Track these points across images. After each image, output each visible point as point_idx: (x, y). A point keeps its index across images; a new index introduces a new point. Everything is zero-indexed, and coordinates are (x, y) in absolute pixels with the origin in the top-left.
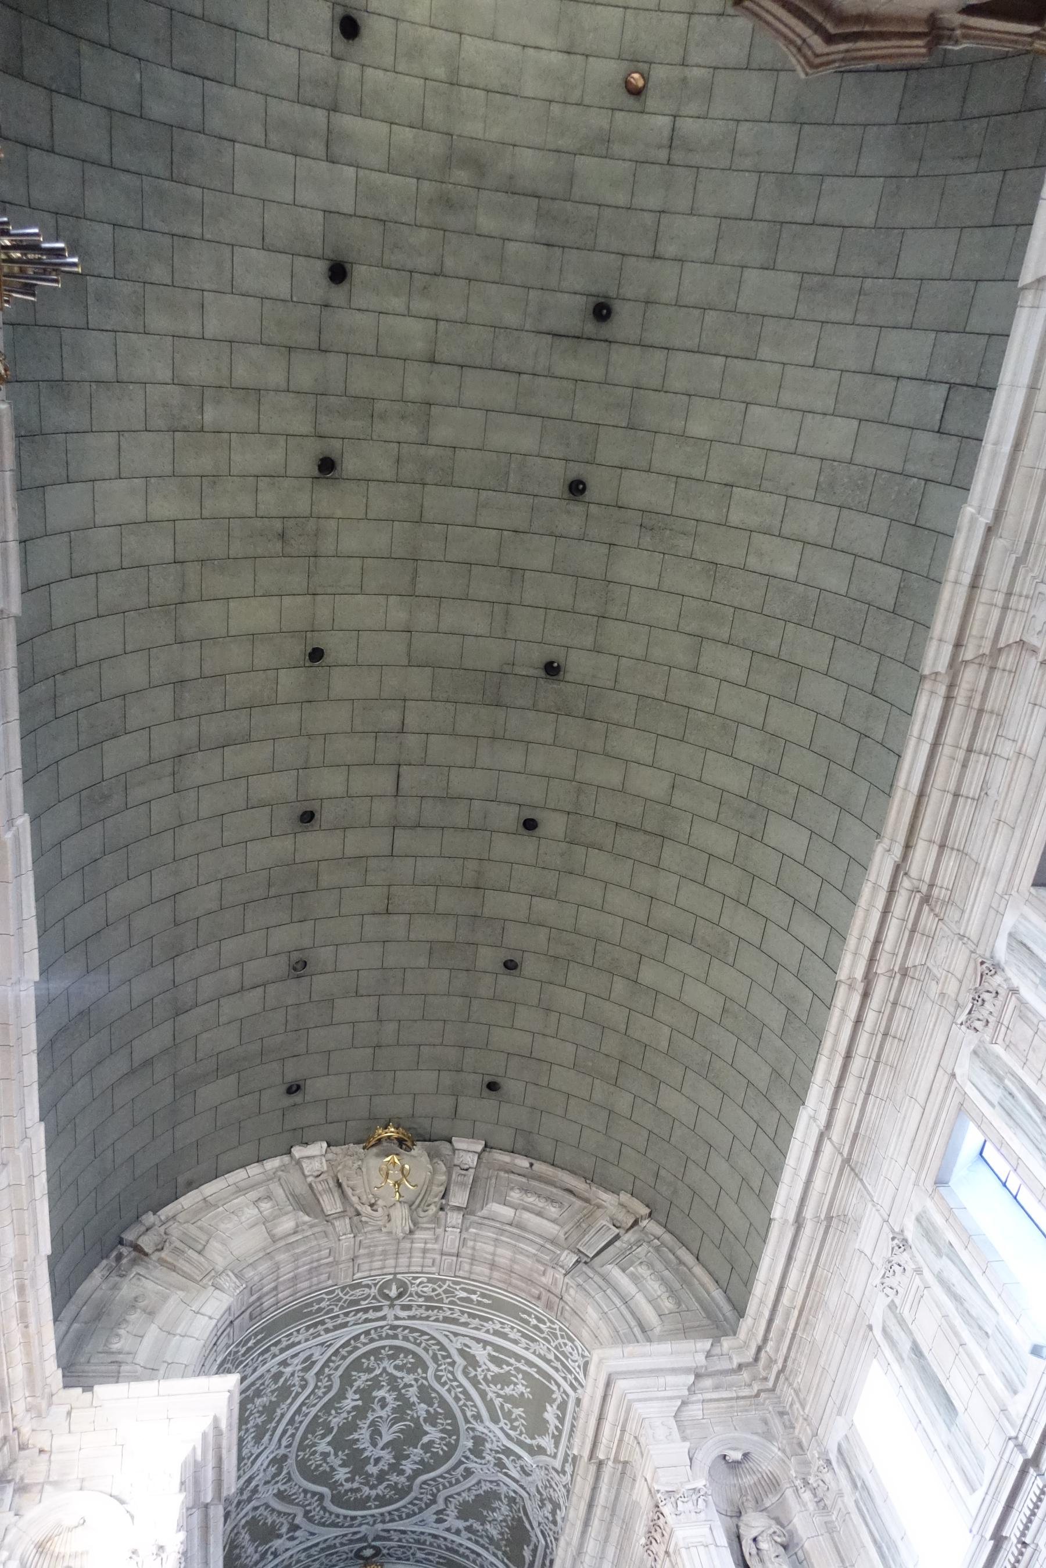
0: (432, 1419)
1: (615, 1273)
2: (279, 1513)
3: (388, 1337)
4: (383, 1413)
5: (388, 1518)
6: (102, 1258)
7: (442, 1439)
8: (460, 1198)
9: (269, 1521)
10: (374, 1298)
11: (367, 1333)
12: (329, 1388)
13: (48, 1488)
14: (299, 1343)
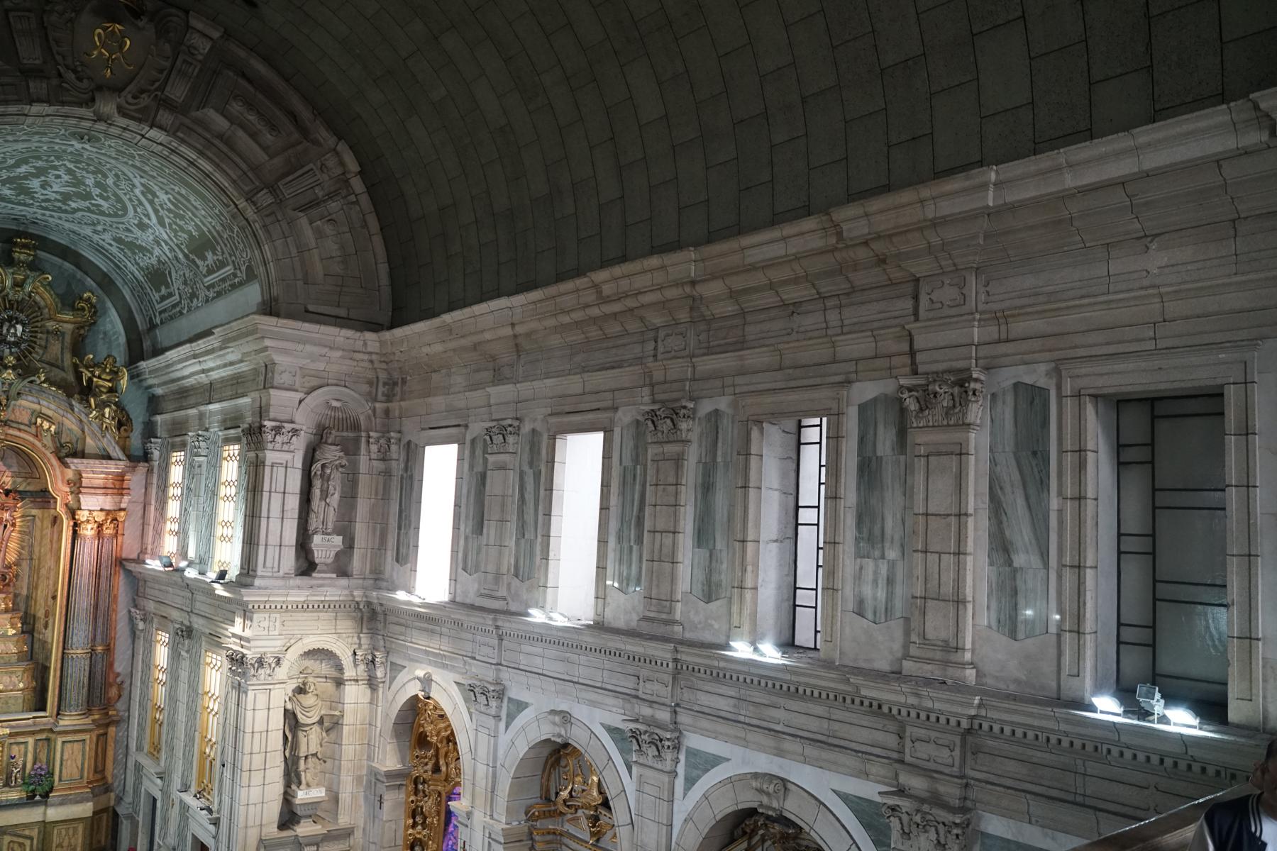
1: (303, 221)
8: (178, 91)
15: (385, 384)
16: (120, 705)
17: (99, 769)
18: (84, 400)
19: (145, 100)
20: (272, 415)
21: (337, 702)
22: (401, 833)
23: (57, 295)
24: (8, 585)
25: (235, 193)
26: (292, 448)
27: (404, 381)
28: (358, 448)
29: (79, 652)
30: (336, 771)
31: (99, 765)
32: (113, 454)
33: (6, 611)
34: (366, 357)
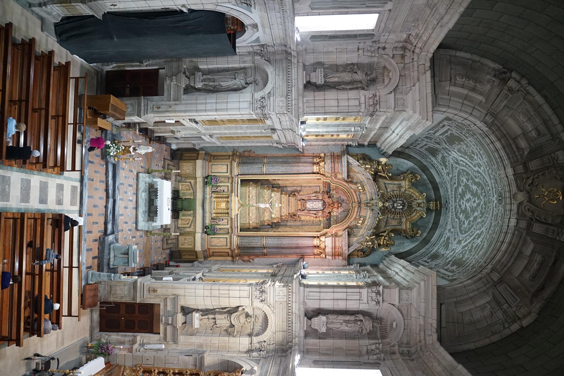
1: (488, 299)
6: (503, 65)
8: (537, 228)
13: (403, 65)
15: (409, 351)
16: (241, 261)
17: (214, 254)
18: (373, 234)
19: (529, 214)
20: (385, 290)
21: (240, 334)
22: (171, 366)
23: (417, 221)
24: (291, 217)
25: (493, 263)
26: (370, 302)
27: (413, 360)
28: (372, 339)
29: (265, 242)
30: (206, 334)
31: (216, 254)
32: (350, 248)
33: (281, 216)
34: (422, 338)
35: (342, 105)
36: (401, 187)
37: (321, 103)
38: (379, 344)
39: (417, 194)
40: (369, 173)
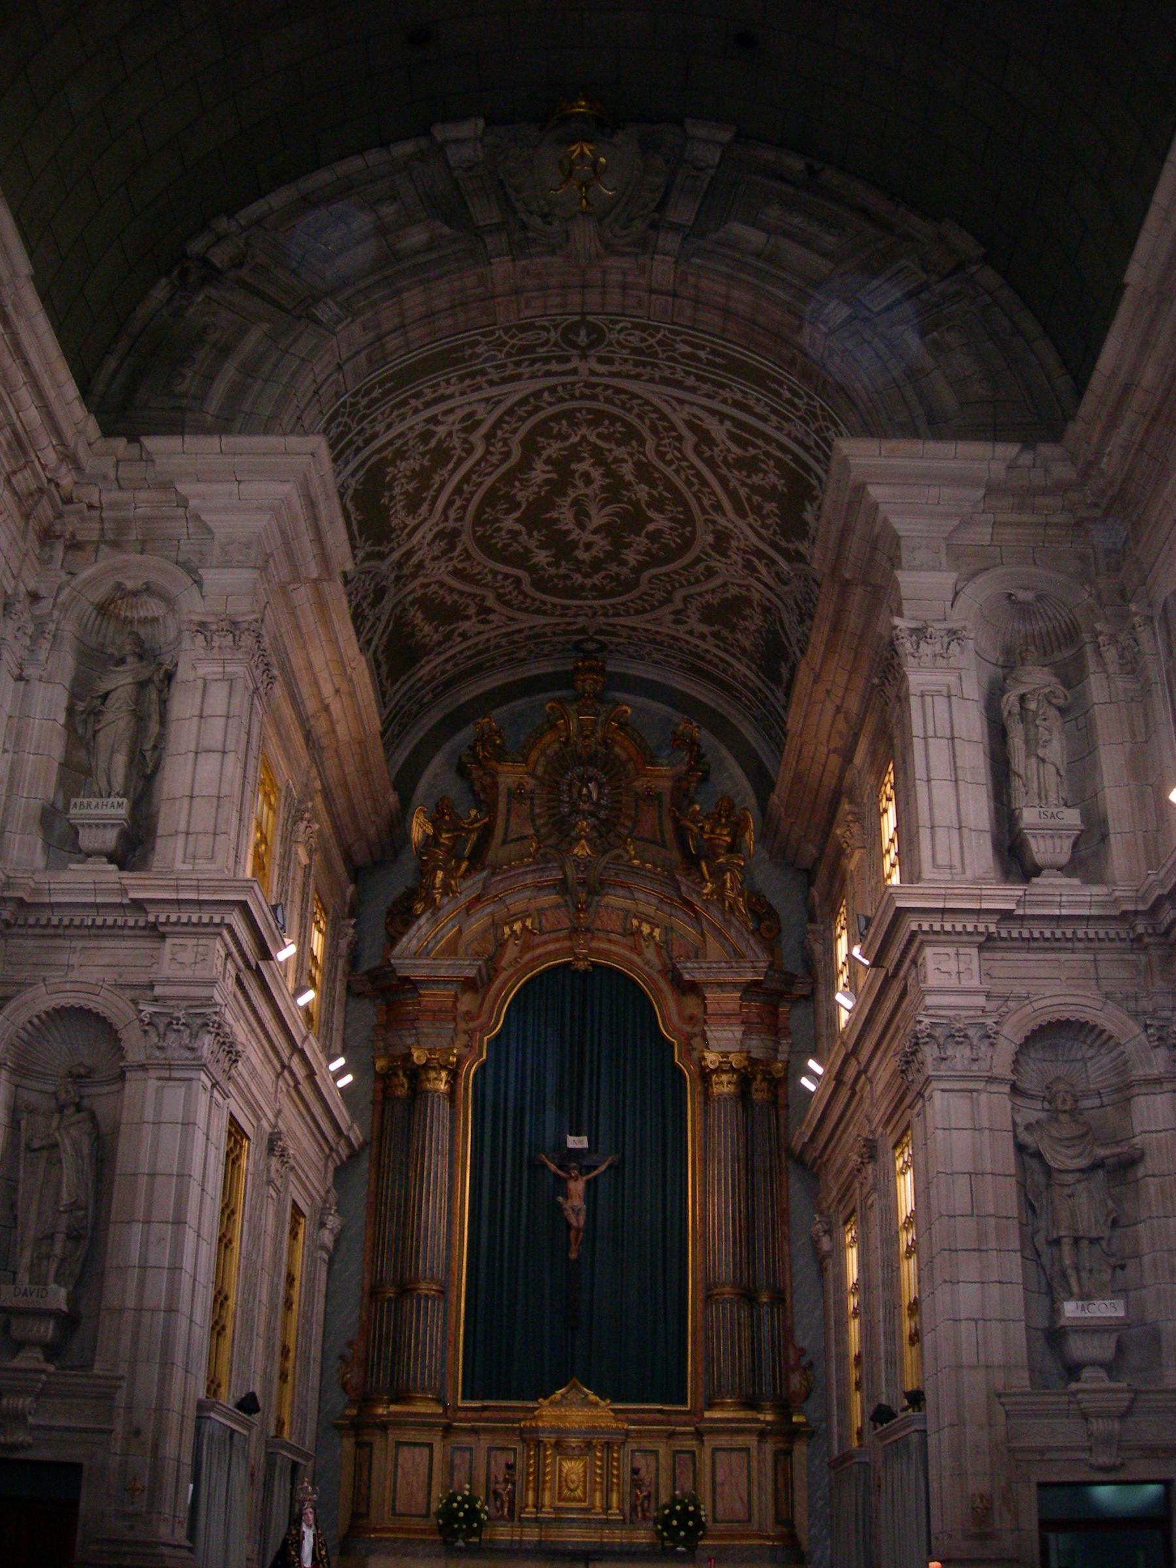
0: (657, 504)
2: (462, 594)
3: (583, 397)
4: (589, 491)
5: (611, 612)
7: (671, 528)
8: (683, 212)
9: (449, 600)
10: (556, 344)
11: (552, 390)
12: (507, 455)
14: (452, 396)
35: (220, 737)
36: (521, 786)
37: (203, 815)
38: (1097, 634)
39: (549, 738)
40: (464, 877)
